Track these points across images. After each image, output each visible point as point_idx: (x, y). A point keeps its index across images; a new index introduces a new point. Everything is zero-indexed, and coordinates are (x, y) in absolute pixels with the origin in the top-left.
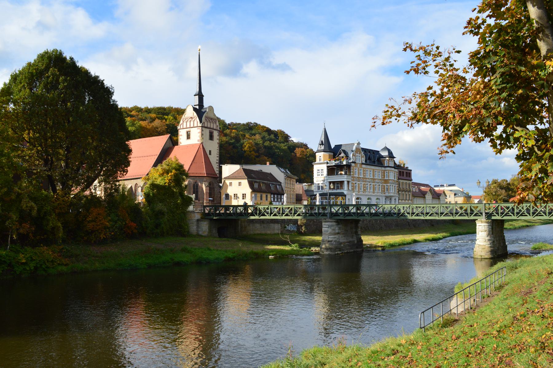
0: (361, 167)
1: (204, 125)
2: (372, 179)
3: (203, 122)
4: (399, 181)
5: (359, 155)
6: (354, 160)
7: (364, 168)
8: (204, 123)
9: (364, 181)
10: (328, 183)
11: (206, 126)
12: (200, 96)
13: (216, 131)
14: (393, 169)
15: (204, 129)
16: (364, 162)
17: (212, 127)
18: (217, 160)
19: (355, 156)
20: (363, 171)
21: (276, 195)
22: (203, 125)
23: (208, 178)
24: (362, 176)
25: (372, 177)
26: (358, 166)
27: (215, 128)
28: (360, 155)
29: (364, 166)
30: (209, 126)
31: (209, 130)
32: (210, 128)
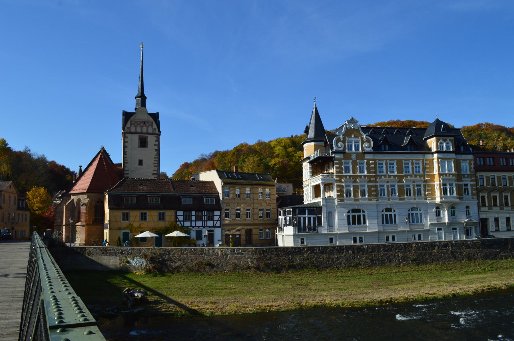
0: (364, 159)
1: (130, 129)
2: (395, 176)
3: (126, 128)
4: (479, 174)
5: (356, 139)
6: (341, 149)
7: (368, 160)
8: (129, 128)
9: (370, 181)
10: (311, 187)
11: (133, 129)
12: (142, 98)
13: (153, 136)
14: (453, 156)
15: (127, 135)
16: (370, 149)
17: (144, 130)
18: (154, 170)
19: (344, 142)
20: (368, 164)
21: (193, 213)
22: (126, 131)
23: (92, 194)
24: (366, 173)
25: (396, 173)
26: (354, 157)
27: (150, 130)
28: (359, 139)
29: (367, 156)
30: (139, 130)
31: (139, 136)
32: (142, 133)
